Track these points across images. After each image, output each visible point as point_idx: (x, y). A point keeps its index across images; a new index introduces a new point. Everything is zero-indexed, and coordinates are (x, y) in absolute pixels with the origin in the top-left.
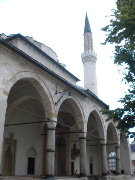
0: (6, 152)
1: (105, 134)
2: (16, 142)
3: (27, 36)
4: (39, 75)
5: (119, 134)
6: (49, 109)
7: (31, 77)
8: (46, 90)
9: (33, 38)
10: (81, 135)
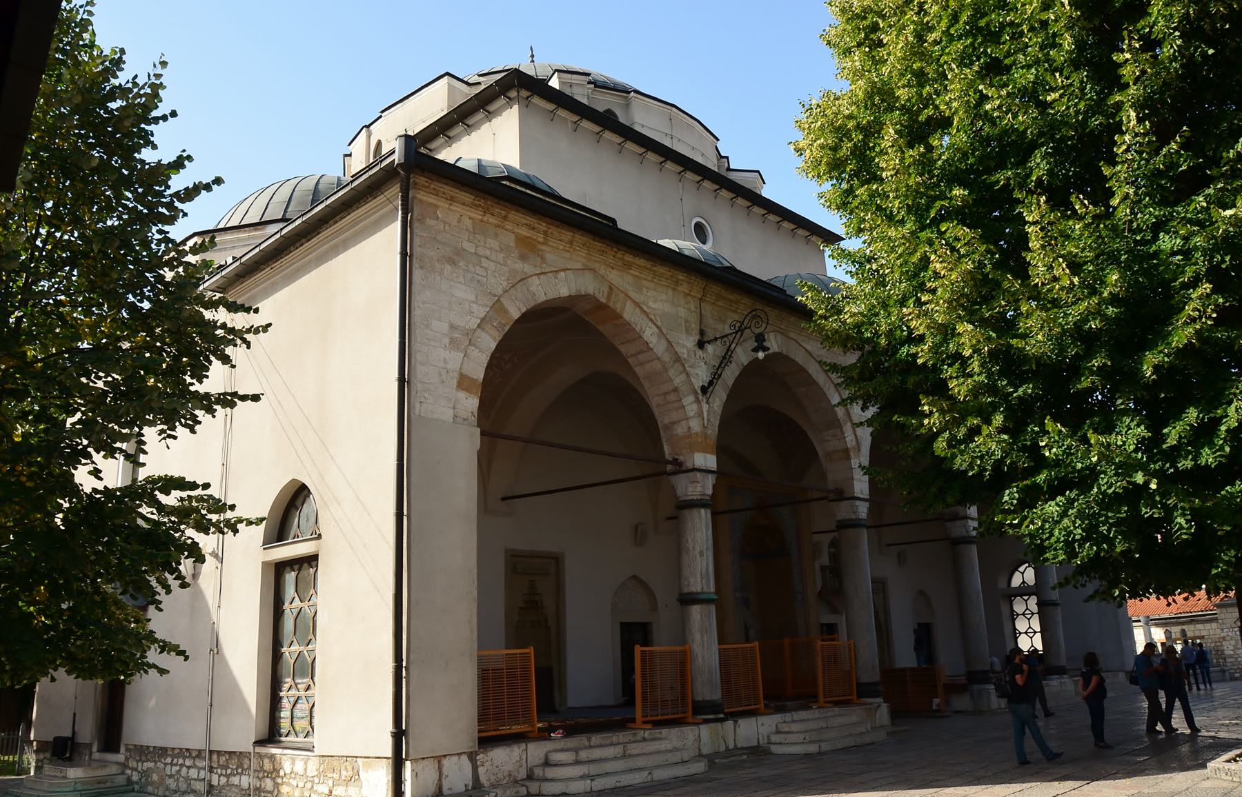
4: (615, 277)
6: (675, 416)
8: (650, 334)
9: (589, 75)
10: (843, 511)
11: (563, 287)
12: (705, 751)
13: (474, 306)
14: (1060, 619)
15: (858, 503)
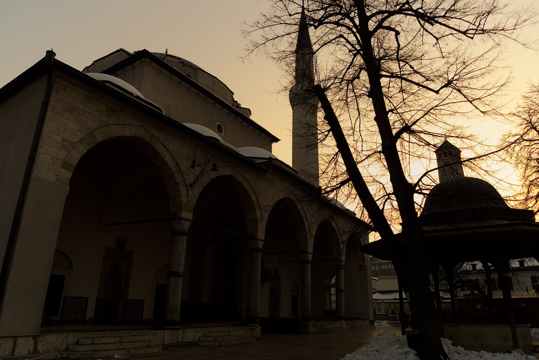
5: (343, 242)
8: (168, 159)
11: (127, 132)
12: (166, 342)
13: (78, 132)
14: (343, 297)
15: (258, 241)
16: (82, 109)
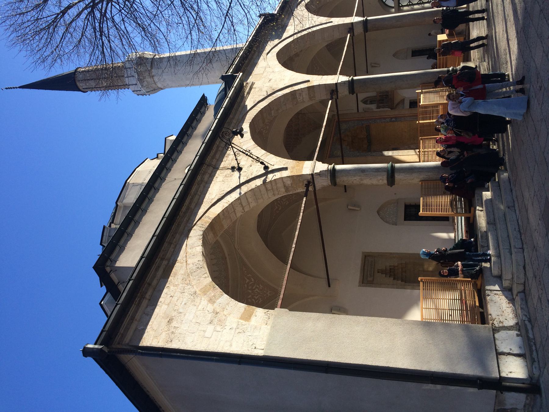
0: (394, 279)
1: (337, 21)
2: (369, 256)
3: (101, 244)
6: (280, 185)
7: (200, 242)
9: (104, 227)
16: (166, 307)
